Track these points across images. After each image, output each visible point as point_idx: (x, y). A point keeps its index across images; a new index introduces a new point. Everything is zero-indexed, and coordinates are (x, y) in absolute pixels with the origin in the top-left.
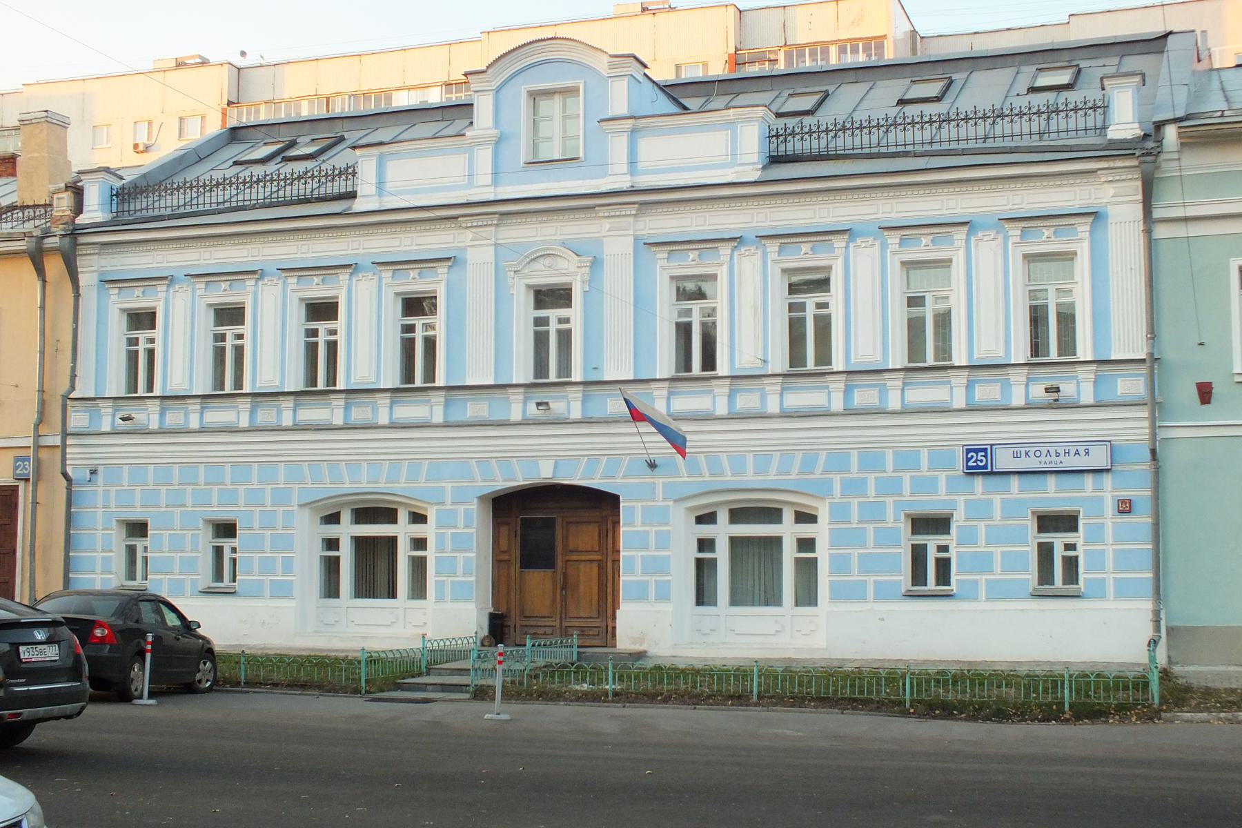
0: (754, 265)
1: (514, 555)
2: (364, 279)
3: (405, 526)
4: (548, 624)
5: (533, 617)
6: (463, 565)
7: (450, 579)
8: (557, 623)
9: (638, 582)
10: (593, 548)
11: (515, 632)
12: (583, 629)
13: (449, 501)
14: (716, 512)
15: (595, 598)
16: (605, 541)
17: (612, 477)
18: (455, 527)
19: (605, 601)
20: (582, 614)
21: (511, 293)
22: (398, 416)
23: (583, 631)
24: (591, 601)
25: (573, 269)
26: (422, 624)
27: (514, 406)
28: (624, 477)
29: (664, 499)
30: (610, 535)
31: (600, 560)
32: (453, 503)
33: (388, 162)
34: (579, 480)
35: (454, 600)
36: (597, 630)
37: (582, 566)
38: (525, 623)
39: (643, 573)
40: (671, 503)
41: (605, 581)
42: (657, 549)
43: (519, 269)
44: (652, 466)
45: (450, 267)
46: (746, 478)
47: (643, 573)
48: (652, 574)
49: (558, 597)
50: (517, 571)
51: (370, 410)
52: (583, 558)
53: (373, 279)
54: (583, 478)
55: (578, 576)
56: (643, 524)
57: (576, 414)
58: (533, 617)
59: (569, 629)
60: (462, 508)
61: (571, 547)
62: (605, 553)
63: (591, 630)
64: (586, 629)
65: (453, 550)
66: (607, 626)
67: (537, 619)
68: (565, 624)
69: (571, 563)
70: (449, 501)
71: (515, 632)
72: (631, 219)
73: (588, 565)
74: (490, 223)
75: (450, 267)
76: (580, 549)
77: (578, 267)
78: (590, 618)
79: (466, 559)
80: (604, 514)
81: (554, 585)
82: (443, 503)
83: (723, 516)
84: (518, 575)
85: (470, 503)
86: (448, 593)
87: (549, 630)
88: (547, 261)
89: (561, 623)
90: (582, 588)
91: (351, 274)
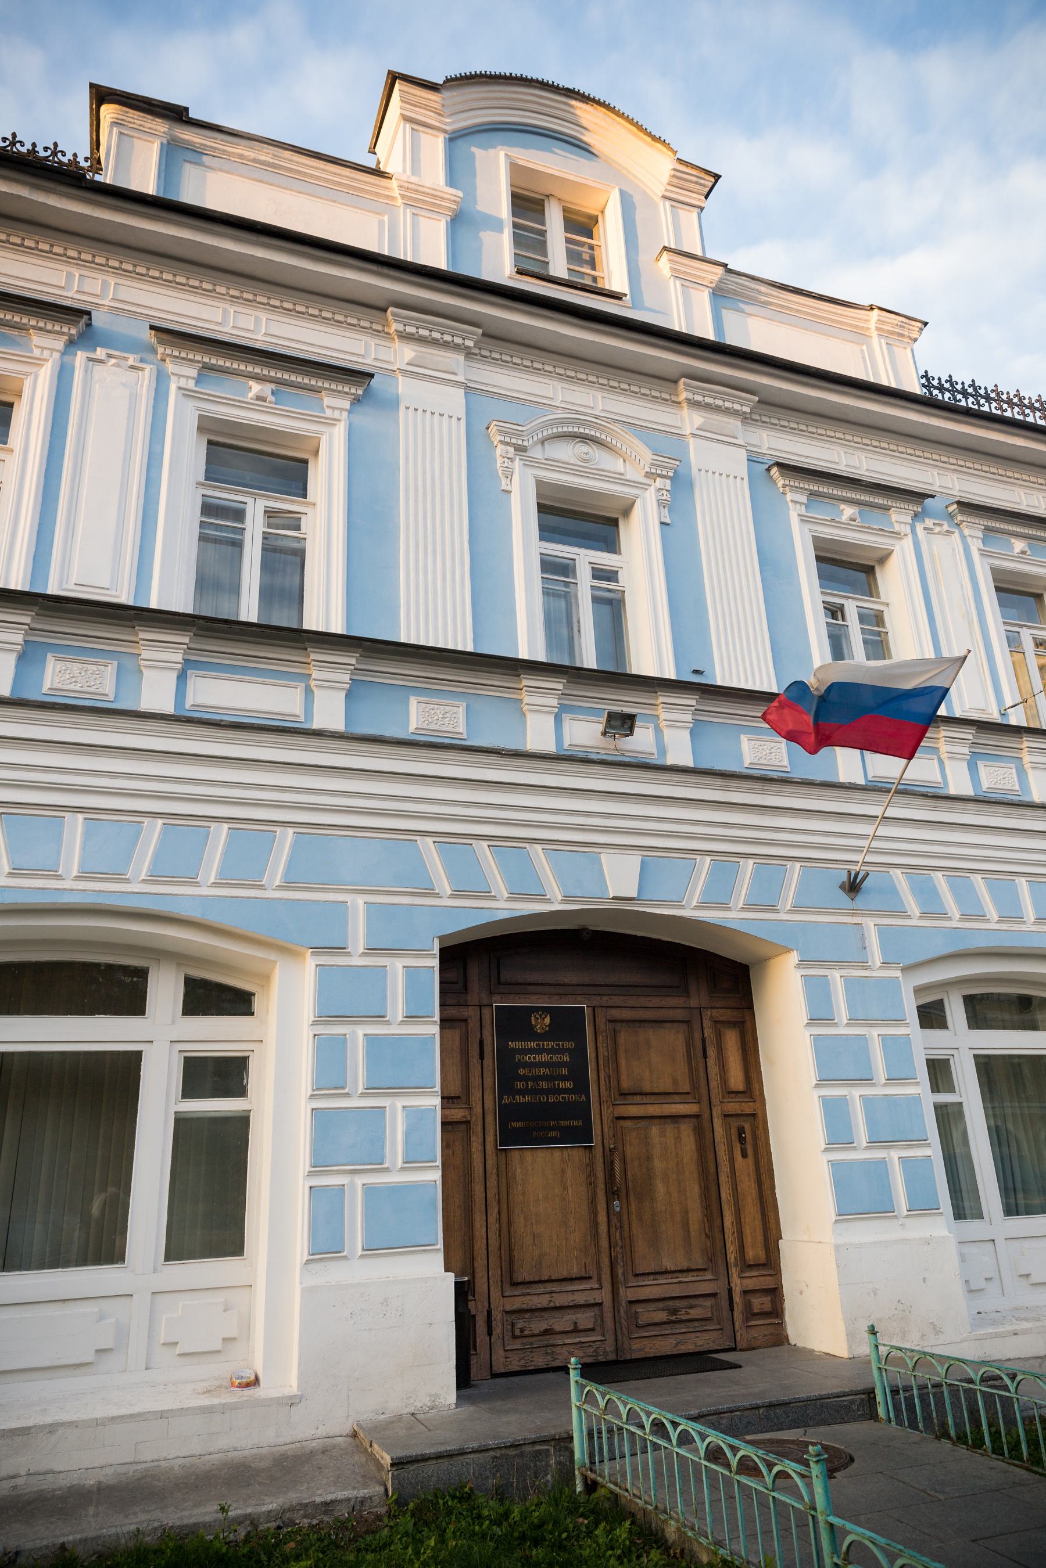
0: (953, 550)
1: (478, 1109)
2: (113, 361)
3: (173, 1022)
4: (580, 1299)
5: (541, 1282)
6: (407, 1135)
7: (360, 1181)
8: (604, 1296)
9: (865, 1162)
10: (675, 1082)
11: (490, 1333)
12: (671, 1303)
13: (358, 941)
14: (942, 1000)
15: (696, 1215)
16: (701, 1060)
17: (772, 908)
18: (379, 1017)
19: (718, 1222)
20: (668, 1264)
21: (504, 487)
22: (201, 701)
23: (674, 1311)
24: (686, 1225)
25: (634, 474)
26: (217, 1345)
27: (532, 719)
28: (796, 909)
29: (886, 964)
30: (711, 1052)
31: (697, 1116)
32: (372, 950)
33: (188, 167)
34: (696, 908)
35: (371, 1250)
36: (709, 1303)
37: (655, 1131)
38: (517, 1303)
39: (874, 1143)
40: (898, 974)
41: (712, 1169)
42: (891, 1080)
43: (525, 443)
44: (853, 886)
45: (357, 401)
46: (1024, 928)
47: (874, 1143)
48: (890, 1143)
49: (602, 1217)
50: (490, 1147)
51: (110, 671)
52: (652, 1110)
53: (141, 369)
54: (703, 906)
55: (649, 1158)
56: (853, 1021)
57: (681, 752)
58: (541, 1282)
59: (640, 1309)
60: (397, 966)
61: (626, 1084)
62: (705, 1099)
63: (691, 1307)
64: (677, 1303)
65: (372, 1089)
66: (730, 1291)
67: (550, 1287)
68: (627, 1294)
69: (628, 1124)
70: (358, 941)
71: (490, 1333)
72: (735, 423)
73: (670, 1128)
74: (458, 340)
75: (357, 401)
76: (647, 1088)
77: (648, 475)
78: (689, 1270)
79: (414, 1116)
80: (693, 1002)
81: (592, 1184)
82: (340, 949)
83: (956, 1012)
84: (491, 1163)
85: (418, 952)
86: (356, 1236)
87: (585, 1319)
88: (582, 448)
89: (615, 1293)
90: (660, 1188)
91: (71, 343)
